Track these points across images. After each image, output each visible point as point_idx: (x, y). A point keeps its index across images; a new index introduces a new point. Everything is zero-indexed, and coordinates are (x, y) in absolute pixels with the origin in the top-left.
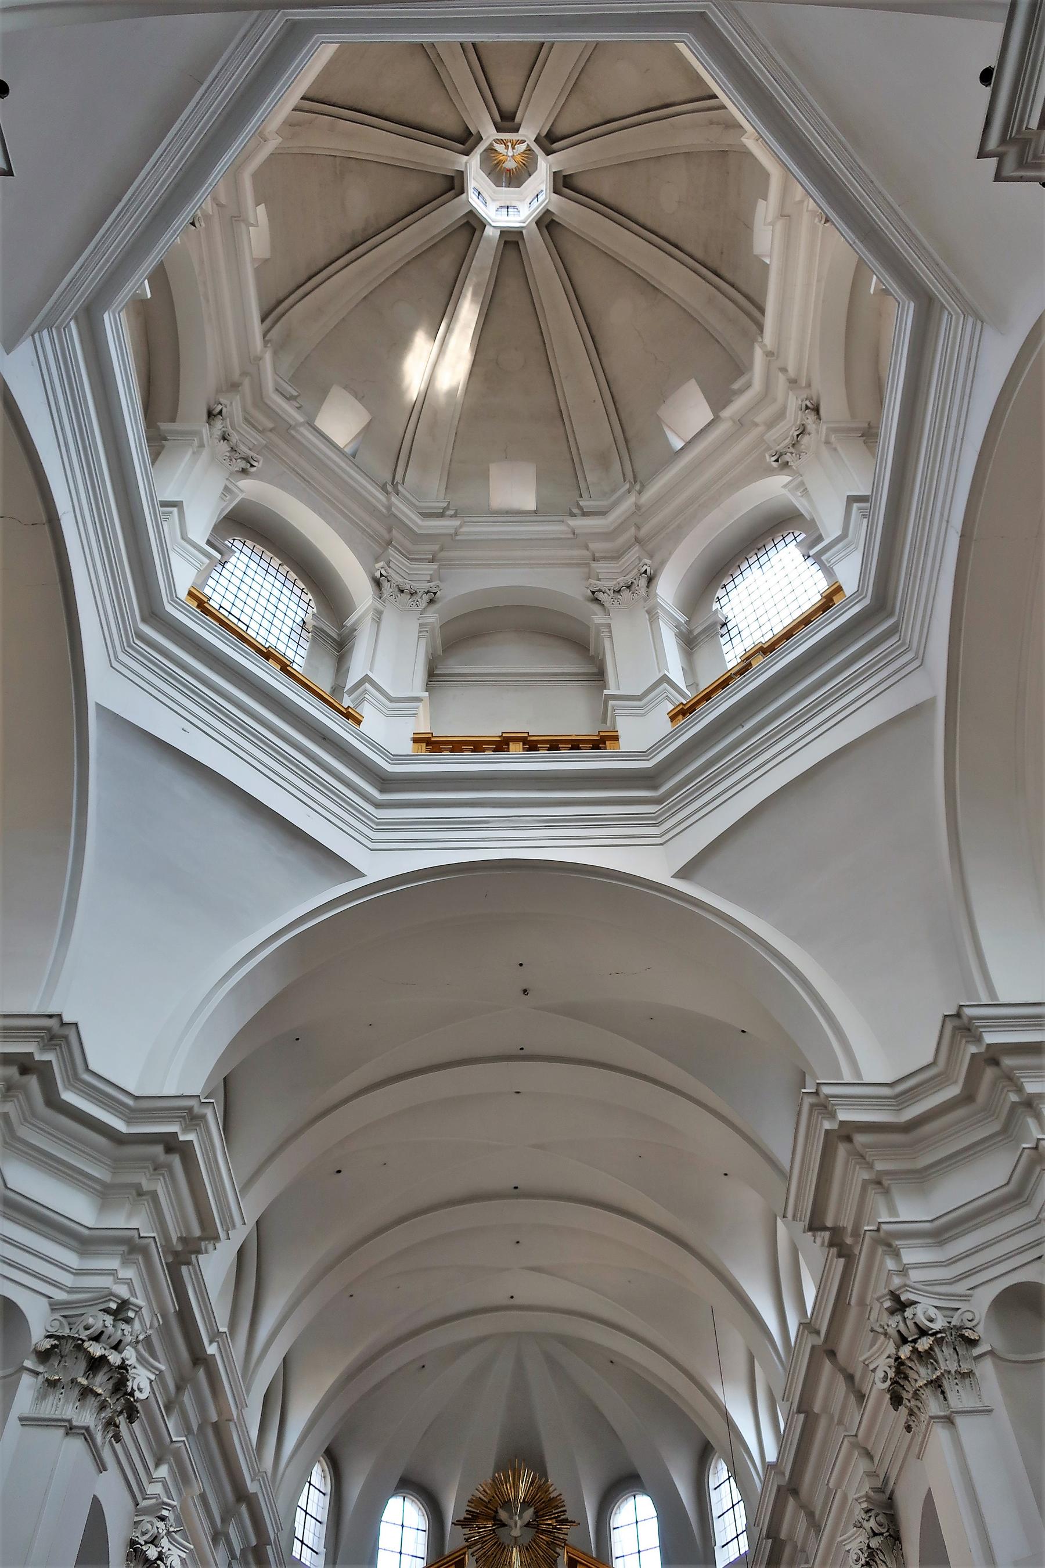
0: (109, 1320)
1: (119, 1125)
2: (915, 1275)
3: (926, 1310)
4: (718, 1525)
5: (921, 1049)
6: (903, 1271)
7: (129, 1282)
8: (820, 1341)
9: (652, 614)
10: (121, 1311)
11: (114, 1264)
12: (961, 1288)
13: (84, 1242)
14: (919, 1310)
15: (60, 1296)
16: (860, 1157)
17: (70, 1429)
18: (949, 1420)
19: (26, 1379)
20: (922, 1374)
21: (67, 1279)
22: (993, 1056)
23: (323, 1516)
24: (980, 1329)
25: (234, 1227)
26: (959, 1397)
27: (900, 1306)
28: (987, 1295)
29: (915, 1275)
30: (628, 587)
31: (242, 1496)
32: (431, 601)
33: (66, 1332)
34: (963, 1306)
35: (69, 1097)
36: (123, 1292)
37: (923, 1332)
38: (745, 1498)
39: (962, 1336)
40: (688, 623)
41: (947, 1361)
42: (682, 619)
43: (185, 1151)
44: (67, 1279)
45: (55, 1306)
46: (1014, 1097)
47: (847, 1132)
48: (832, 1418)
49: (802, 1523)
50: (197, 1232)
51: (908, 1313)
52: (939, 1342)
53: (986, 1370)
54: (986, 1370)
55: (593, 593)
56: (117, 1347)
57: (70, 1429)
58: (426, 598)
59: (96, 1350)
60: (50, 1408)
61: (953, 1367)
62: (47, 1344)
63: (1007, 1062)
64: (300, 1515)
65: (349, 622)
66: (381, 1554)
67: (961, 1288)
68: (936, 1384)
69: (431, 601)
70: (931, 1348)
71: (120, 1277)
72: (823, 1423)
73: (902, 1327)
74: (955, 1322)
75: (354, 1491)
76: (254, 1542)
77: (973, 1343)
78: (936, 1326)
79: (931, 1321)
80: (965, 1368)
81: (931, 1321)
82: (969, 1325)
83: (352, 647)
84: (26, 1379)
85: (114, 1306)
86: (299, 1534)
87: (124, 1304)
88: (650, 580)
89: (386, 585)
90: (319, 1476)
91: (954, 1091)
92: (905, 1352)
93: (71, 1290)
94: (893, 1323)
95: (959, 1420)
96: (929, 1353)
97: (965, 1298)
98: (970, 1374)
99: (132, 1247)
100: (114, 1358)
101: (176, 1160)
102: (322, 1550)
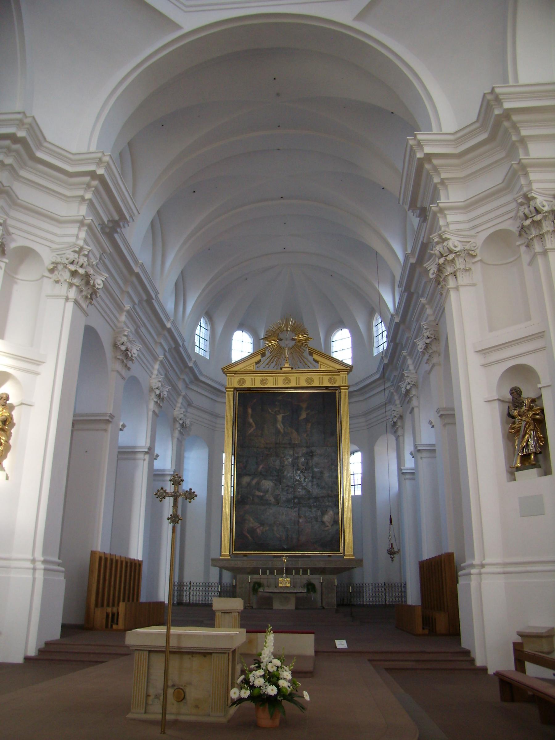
2: (452, 227)
3: (454, 243)
4: (375, 340)
6: (448, 224)
18: (457, 288)
23: (208, 338)
24: (478, 251)
25: (134, 215)
26: (463, 279)
28: (484, 236)
34: (472, 240)
35: (40, 154)
37: (451, 252)
39: (469, 254)
41: (460, 264)
48: (419, 293)
50: (117, 218)
51: (445, 244)
52: (458, 256)
61: (462, 267)
64: (197, 338)
66: (233, 351)
67: (473, 233)
68: (454, 274)
70: (453, 259)
73: (441, 250)
74: (467, 247)
75: (219, 329)
76: (173, 346)
77: (474, 256)
78: (457, 250)
79: (456, 247)
80: (468, 267)
81: (456, 247)
82: (473, 249)
85: (77, 249)
86: (197, 344)
95: (461, 289)
96: (453, 260)
98: (469, 270)
102: (208, 350)
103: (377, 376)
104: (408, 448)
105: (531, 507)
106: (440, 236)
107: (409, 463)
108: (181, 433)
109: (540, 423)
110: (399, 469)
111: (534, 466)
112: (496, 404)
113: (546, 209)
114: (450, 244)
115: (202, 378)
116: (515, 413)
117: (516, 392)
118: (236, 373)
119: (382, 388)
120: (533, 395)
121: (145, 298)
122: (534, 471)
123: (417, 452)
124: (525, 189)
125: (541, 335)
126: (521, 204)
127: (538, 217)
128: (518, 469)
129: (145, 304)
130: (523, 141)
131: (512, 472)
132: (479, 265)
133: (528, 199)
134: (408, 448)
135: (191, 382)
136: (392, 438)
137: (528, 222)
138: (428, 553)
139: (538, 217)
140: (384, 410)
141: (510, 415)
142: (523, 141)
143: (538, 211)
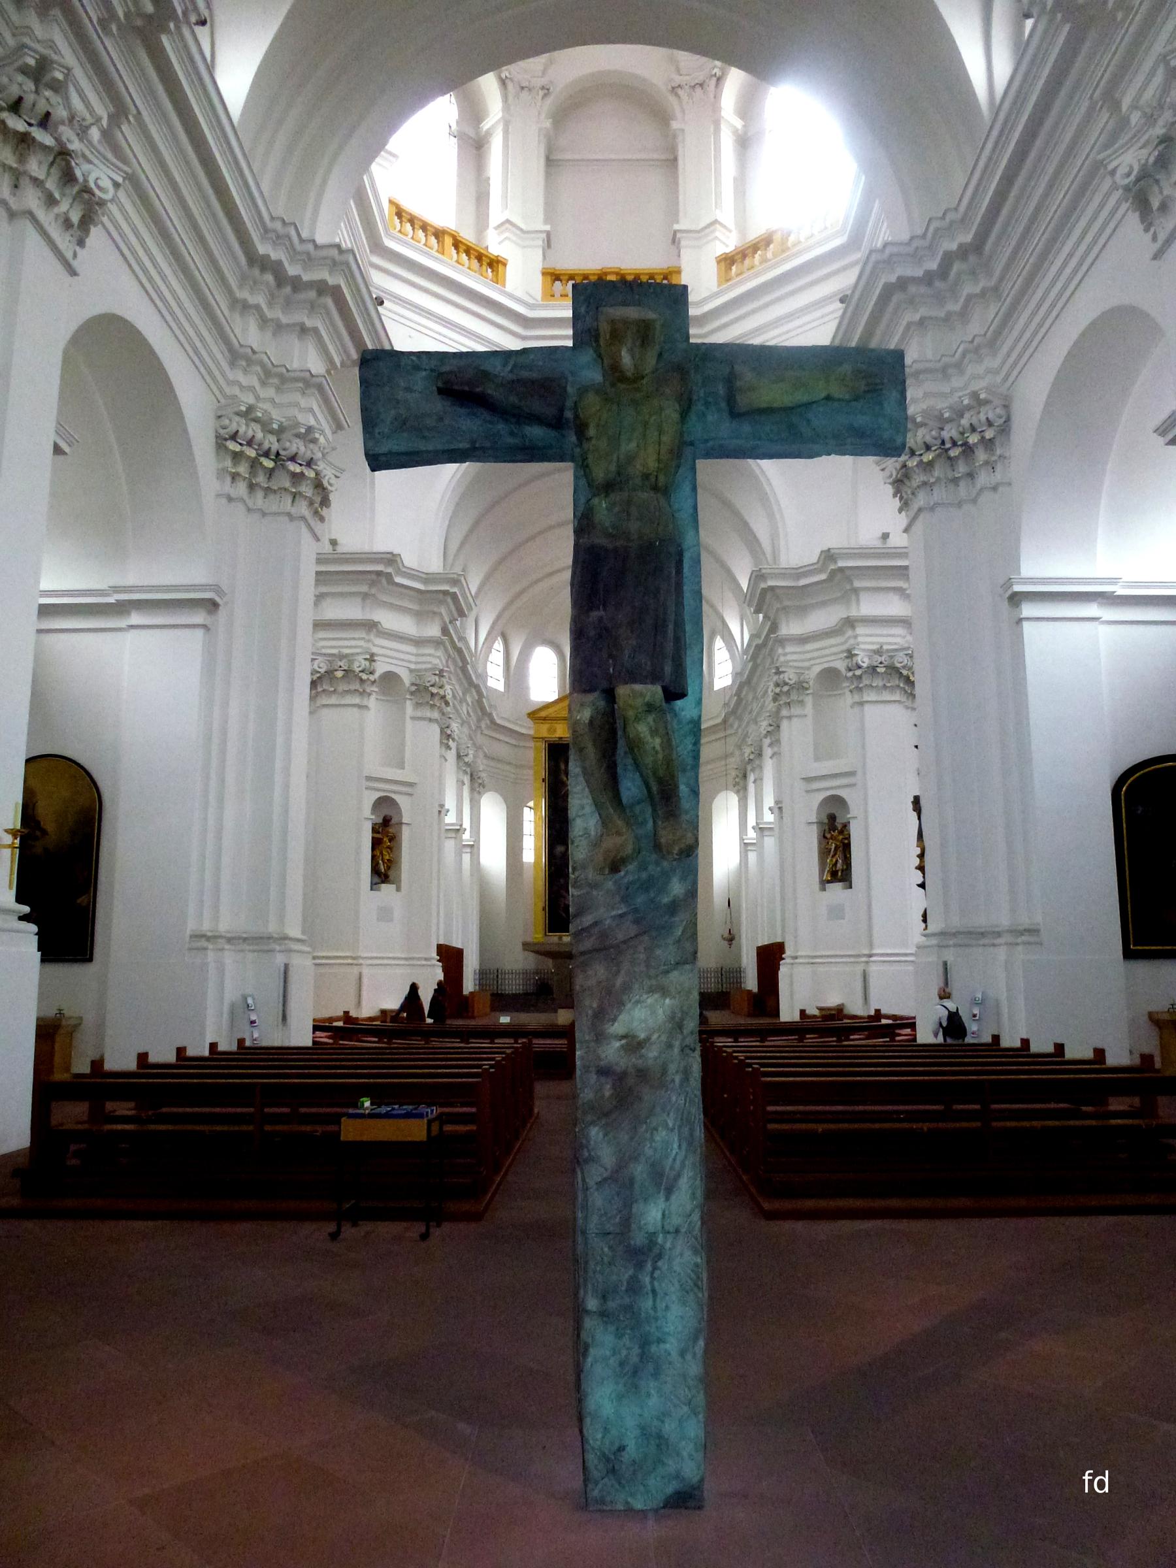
0: (437, 678)
1: (421, 587)
3: (790, 676)
5: (812, 557)
7: (439, 657)
8: (760, 641)
9: (717, 123)
10: (441, 674)
11: (431, 651)
12: (806, 664)
13: (419, 642)
14: (786, 675)
15: (413, 666)
16: (777, 598)
17: (430, 720)
19: (408, 702)
20: (784, 699)
21: (413, 659)
22: (841, 570)
24: (811, 683)
26: (796, 710)
27: (778, 672)
28: (817, 669)
29: (789, 657)
30: (701, 85)
31: (471, 683)
32: (545, 95)
33: (418, 682)
35: (398, 580)
36: (437, 661)
37: (786, 684)
38: (732, 657)
40: (744, 126)
42: (739, 124)
43: (454, 596)
44: (413, 659)
45: (411, 671)
46: (848, 587)
47: (772, 588)
49: (750, 697)
50: (456, 615)
53: (809, 700)
54: (809, 700)
55: (673, 88)
56: (441, 687)
57: (430, 720)
58: (541, 93)
59: (434, 690)
60: (419, 714)
62: (413, 688)
63: (848, 573)
65: (486, 125)
69: (545, 95)
71: (436, 658)
72: (760, 668)
77: (807, 689)
83: (489, 148)
84: (408, 702)
87: (441, 671)
88: (719, 79)
89: (510, 86)
90: (499, 645)
91: (823, 577)
92: (778, 690)
93: (416, 663)
94: (775, 678)
97: (809, 668)
99: (437, 643)
100: (442, 692)
101: (449, 600)
103: (719, 720)
104: (751, 821)
105: (836, 913)
106: (777, 668)
107: (751, 834)
108: (472, 790)
109: (846, 847)
110: (741, 839)
111: (840, 881)
112: (815, 827)
113: (865, 665)
114: (785, 677)
115: (499, 721)
116: (828, 836)
117: (832, 818)
118: (545, 719)
119: (721, 734)
120: (844, 821)
121: (460, 664)
122: (836, 888)
123: (761, 830)
124: (852, 641)
125: (852, 774)
126: (847, 657)
127: (858, 672)
128: (829, 882)
129: (460, 672)
130: (856, 591)
131: (823, 884)
132: (810, 697)
133: (850, 655)
134: (751, 821)
135: (488, 727)
136: (733, 799)
137: (850, 674)
138: (764, 941)
139: (858, 672)
140: (723, 763)
141: (824, 837)
142: (856, 591)
143: (859, 667)
